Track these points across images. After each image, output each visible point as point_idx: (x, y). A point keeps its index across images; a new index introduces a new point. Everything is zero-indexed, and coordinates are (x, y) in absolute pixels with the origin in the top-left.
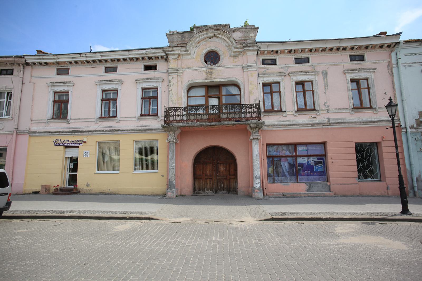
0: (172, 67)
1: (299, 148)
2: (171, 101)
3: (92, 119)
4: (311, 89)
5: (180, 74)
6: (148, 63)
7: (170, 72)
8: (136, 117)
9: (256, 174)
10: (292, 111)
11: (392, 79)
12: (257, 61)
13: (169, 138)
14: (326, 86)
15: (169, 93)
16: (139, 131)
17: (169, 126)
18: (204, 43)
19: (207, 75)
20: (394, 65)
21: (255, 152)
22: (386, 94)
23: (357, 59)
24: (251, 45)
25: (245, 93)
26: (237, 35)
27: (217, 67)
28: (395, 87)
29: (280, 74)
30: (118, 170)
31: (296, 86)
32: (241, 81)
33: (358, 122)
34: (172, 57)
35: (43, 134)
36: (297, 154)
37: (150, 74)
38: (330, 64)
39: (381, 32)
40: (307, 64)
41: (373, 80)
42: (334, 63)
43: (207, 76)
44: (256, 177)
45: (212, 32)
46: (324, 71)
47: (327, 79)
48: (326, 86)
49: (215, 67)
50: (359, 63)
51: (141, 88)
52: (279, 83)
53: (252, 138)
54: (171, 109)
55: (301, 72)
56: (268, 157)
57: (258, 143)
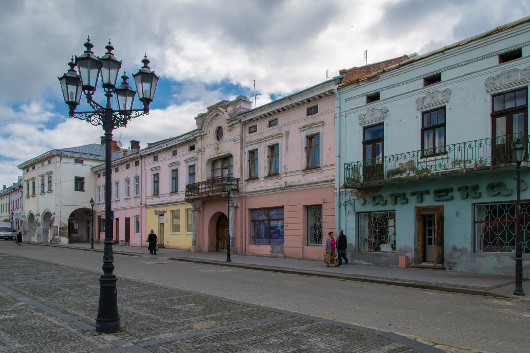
1: (272, 213)
14: (287, 147)
23: (313, 112)
47: (288, 140)
50: (312, 116)
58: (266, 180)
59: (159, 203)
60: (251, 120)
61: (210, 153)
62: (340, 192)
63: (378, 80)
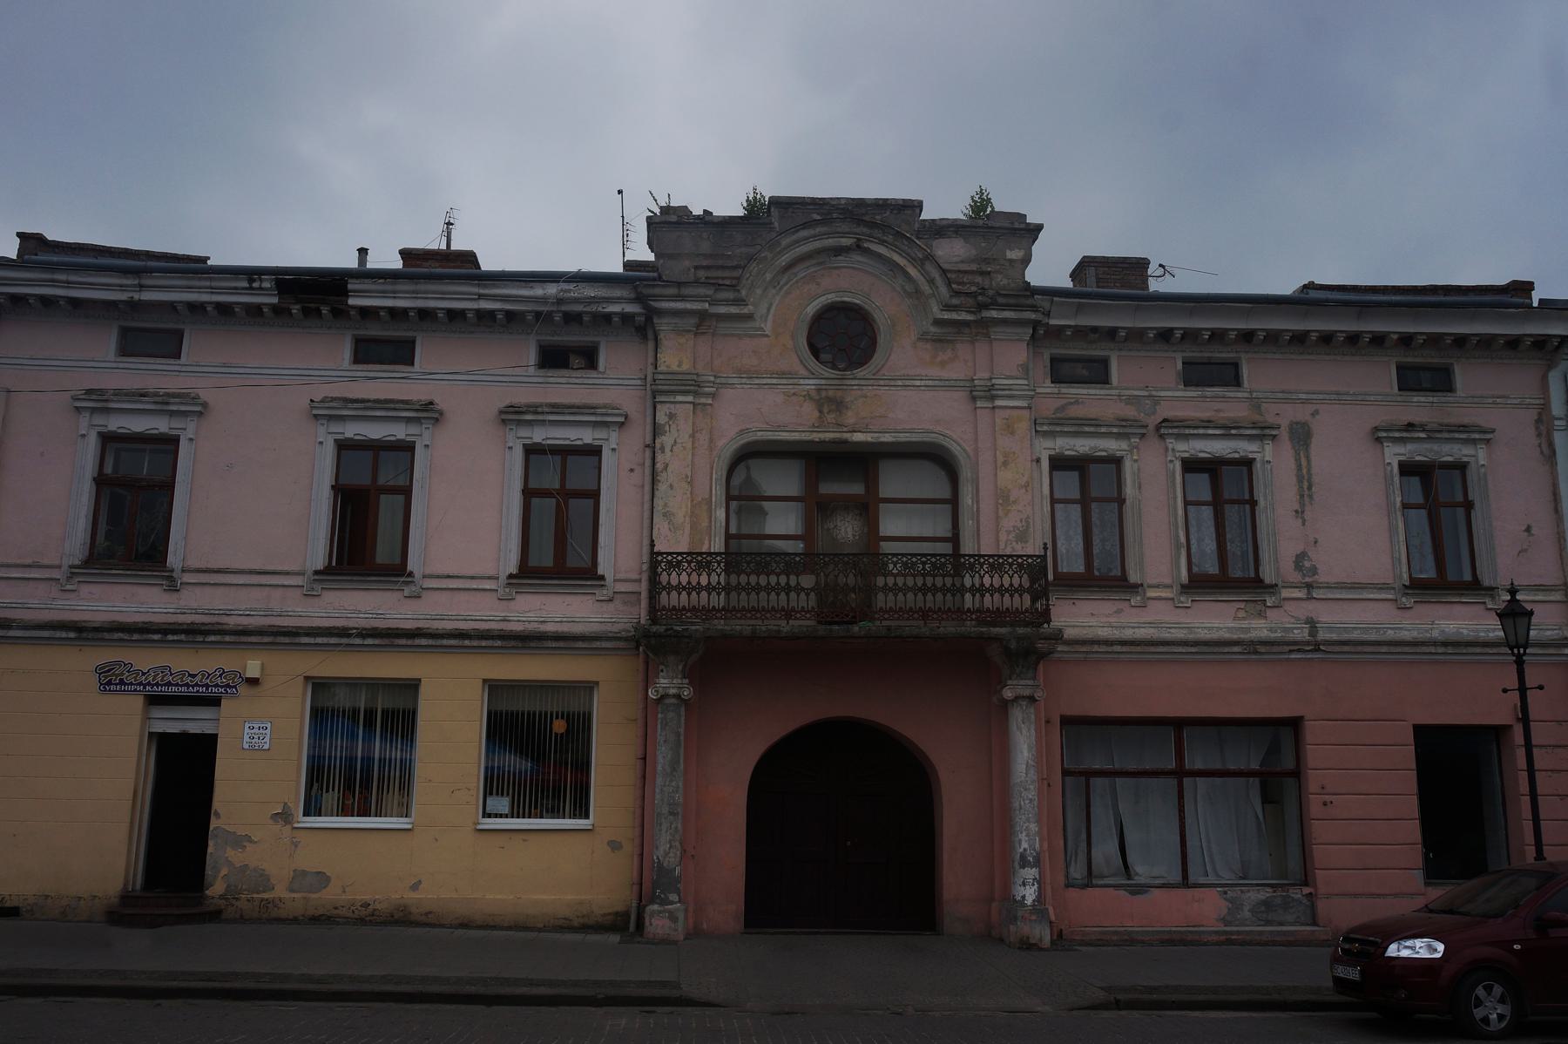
0: (667, 367)
2: (665, 515)
3: (287, 573)
4: (1247, 497)
5: (703, 400)
6: (556, 338)
7: (658, 390)
8: (497, 578)
9: (1025, 845)
10: (1166, 586)
11: (1552, 473)
12: (1031, 366)
13: (662, 681)
15: (654, 481)
16: (513, 643)
17: (669, 632)
18: (812, 270)
19: (821, 412)
20: (1556, 423)
21: (1022, 752)
22: (1533, 535)
24: (1012, 301)
25: (978, 502)
26: (951, 251)
27: (863, 382)
28: (1561, 507)
29: (1125, 428)
31: (1187, 475)
32: (964, 450)
33: (1423, 643)
34: (674, 321)
35: (46, 634)
36: (1187, 767)
37: (566, 388)
38: (1321, 397)
39: (1514, 282)
40: (1231, 392)
41: (1485, 474)
42: (1338, 394)
43: (820, 417)
44: (1023, 856)
45: (847, 230)
46: (1297, 423)
48: (1306, 484)
49: (855, 379)
50: (1431, 399)
51: (524, 444)
52: (1116, 461)
53: (1008, 694)
54: (680, 558)
55: (1208, 423)
56: (1065, 773)
57: (1033, 717)
58: (1186, 600)
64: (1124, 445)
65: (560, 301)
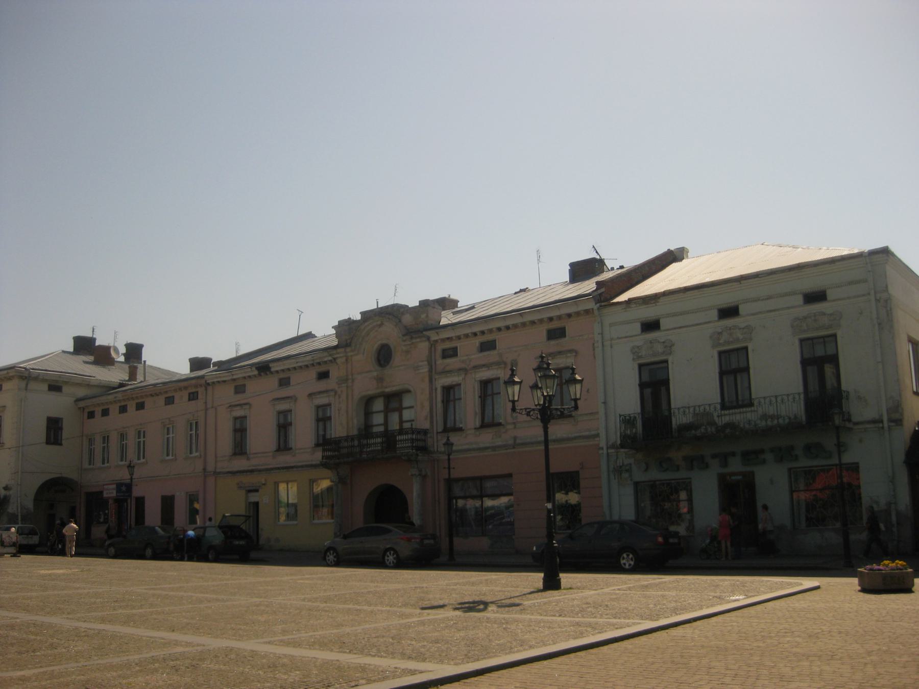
30: (296, 520)
37: (323, 385)
58: (478, 433)
59: (246, 468)
60: (448, 338)
61: (365, 385)
62: (608, 454)
63: (657, 304)
64: (461, 378)
65: (313, 360)
